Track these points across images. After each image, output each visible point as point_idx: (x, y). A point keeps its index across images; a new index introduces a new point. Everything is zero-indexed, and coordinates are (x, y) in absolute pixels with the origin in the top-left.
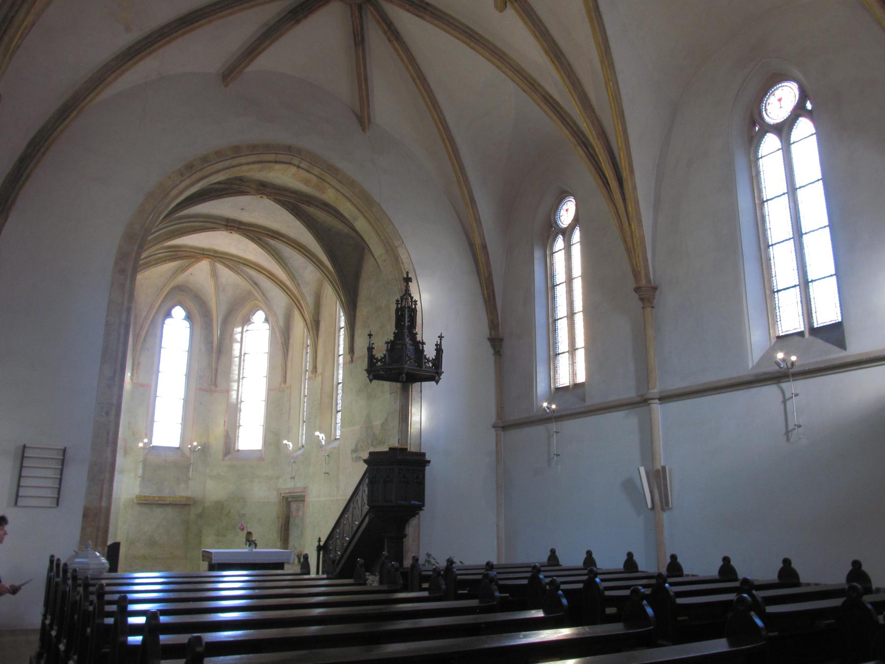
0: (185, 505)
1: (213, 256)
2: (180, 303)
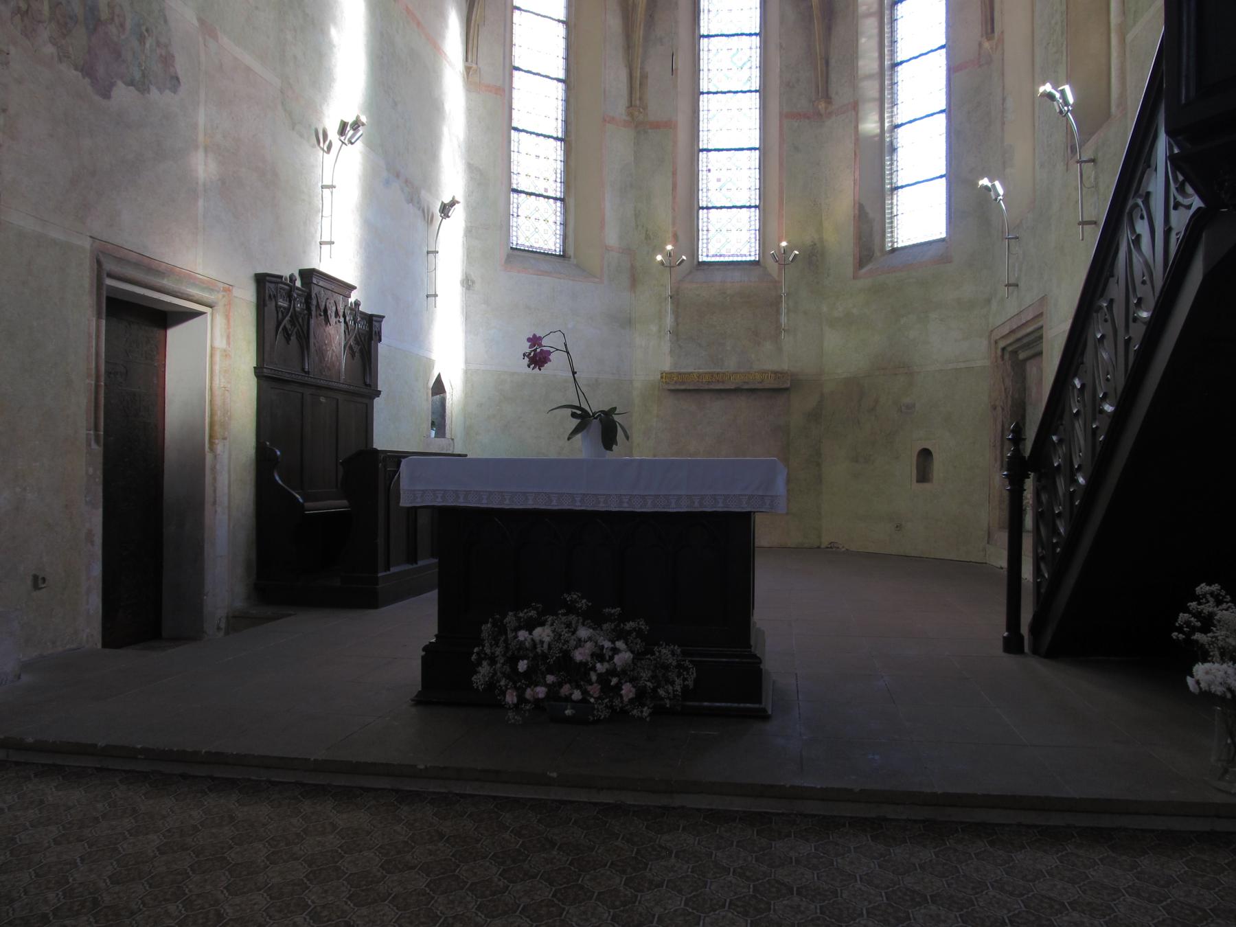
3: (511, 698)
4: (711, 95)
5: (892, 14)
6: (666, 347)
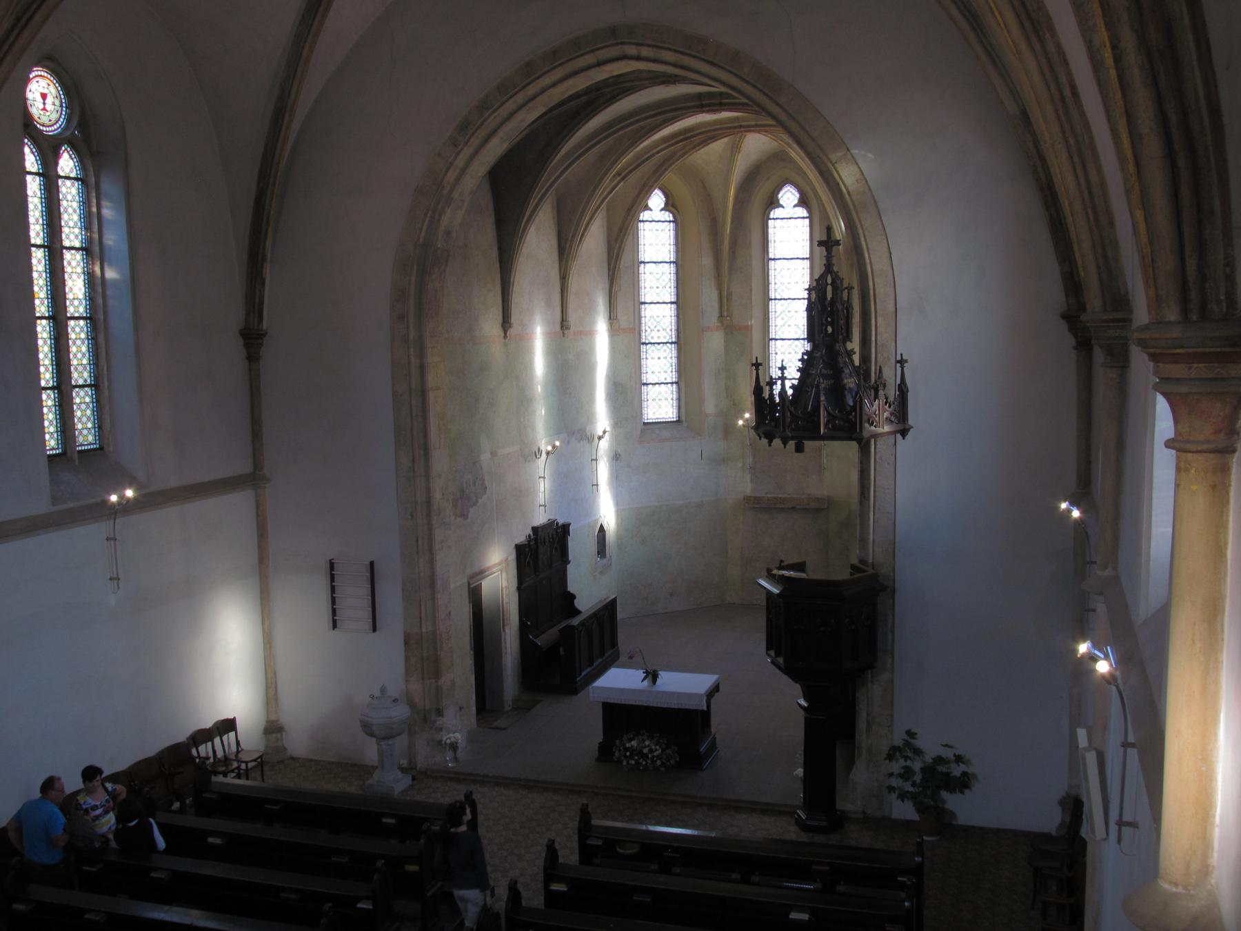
0: (818, 510)
1: (756, 126)
2: (787, 179)
3: (625, 763)
4: (777, 301)
6: (748, 477)
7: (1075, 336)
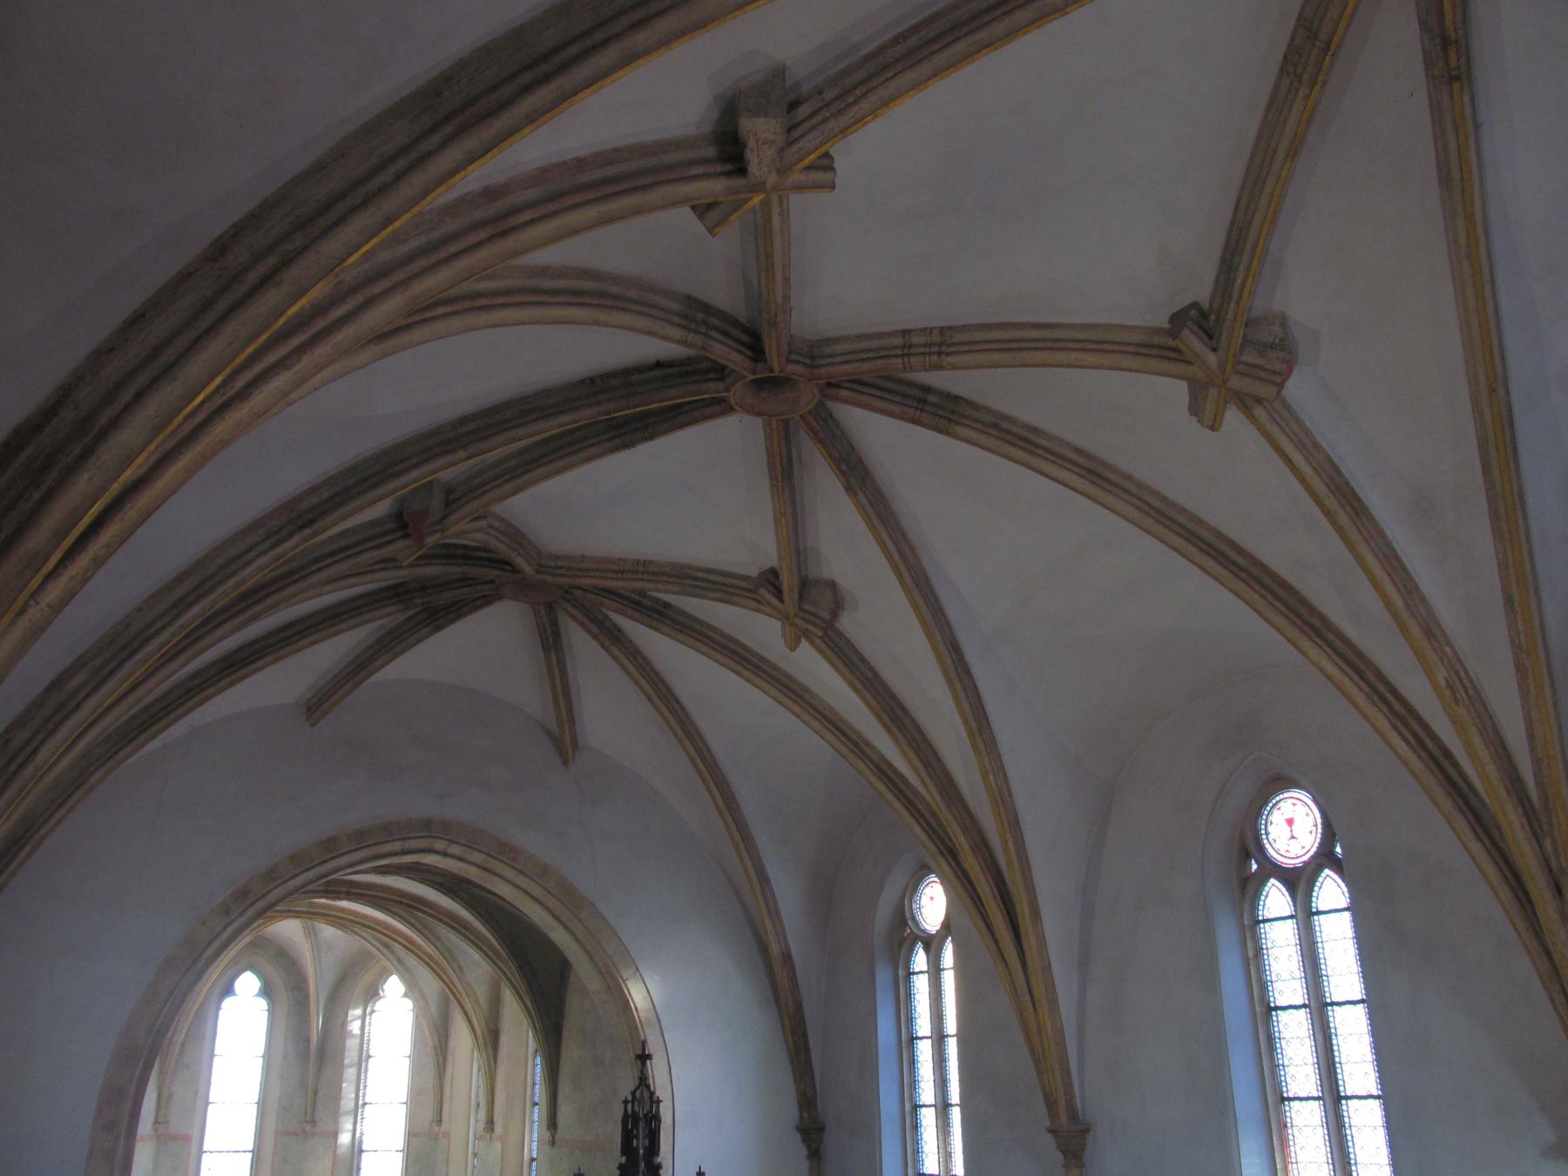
1: (306, 912)
5: (367, 1065)
7: (809, 1147)
